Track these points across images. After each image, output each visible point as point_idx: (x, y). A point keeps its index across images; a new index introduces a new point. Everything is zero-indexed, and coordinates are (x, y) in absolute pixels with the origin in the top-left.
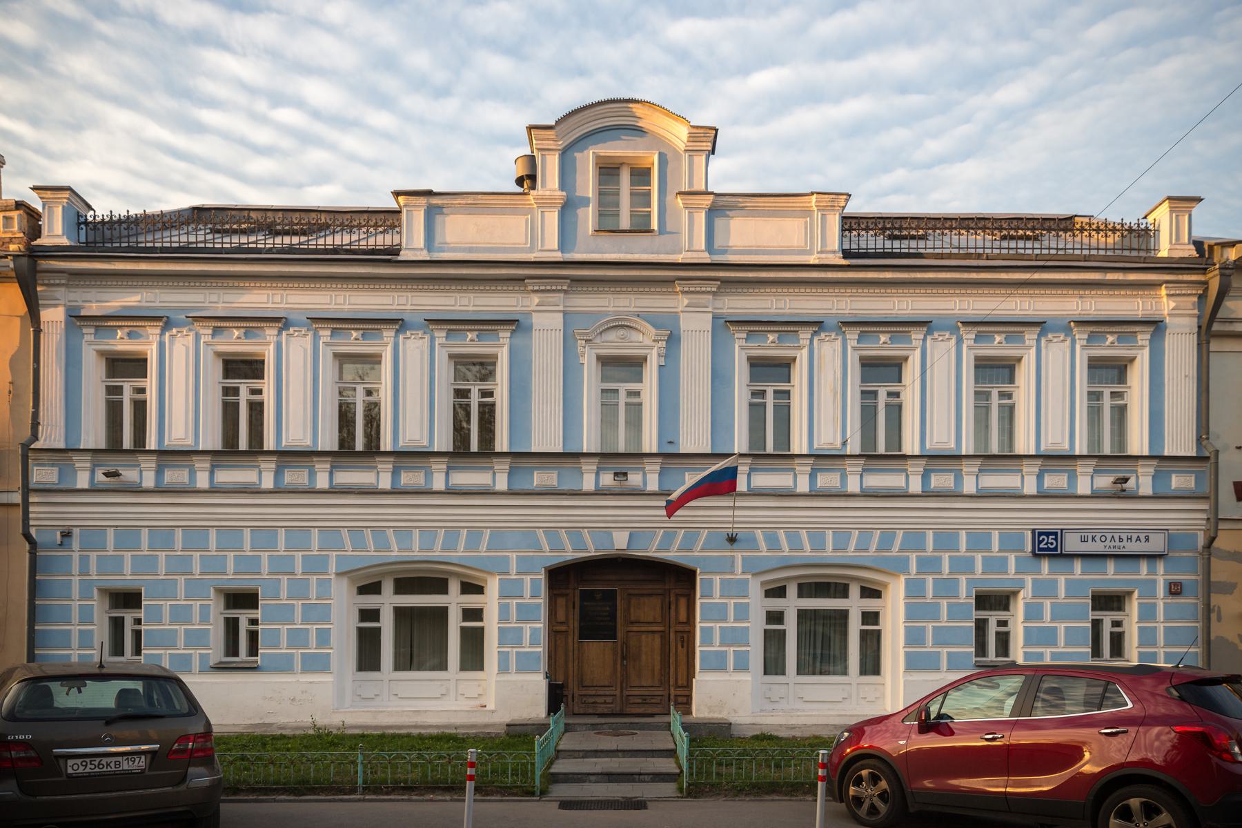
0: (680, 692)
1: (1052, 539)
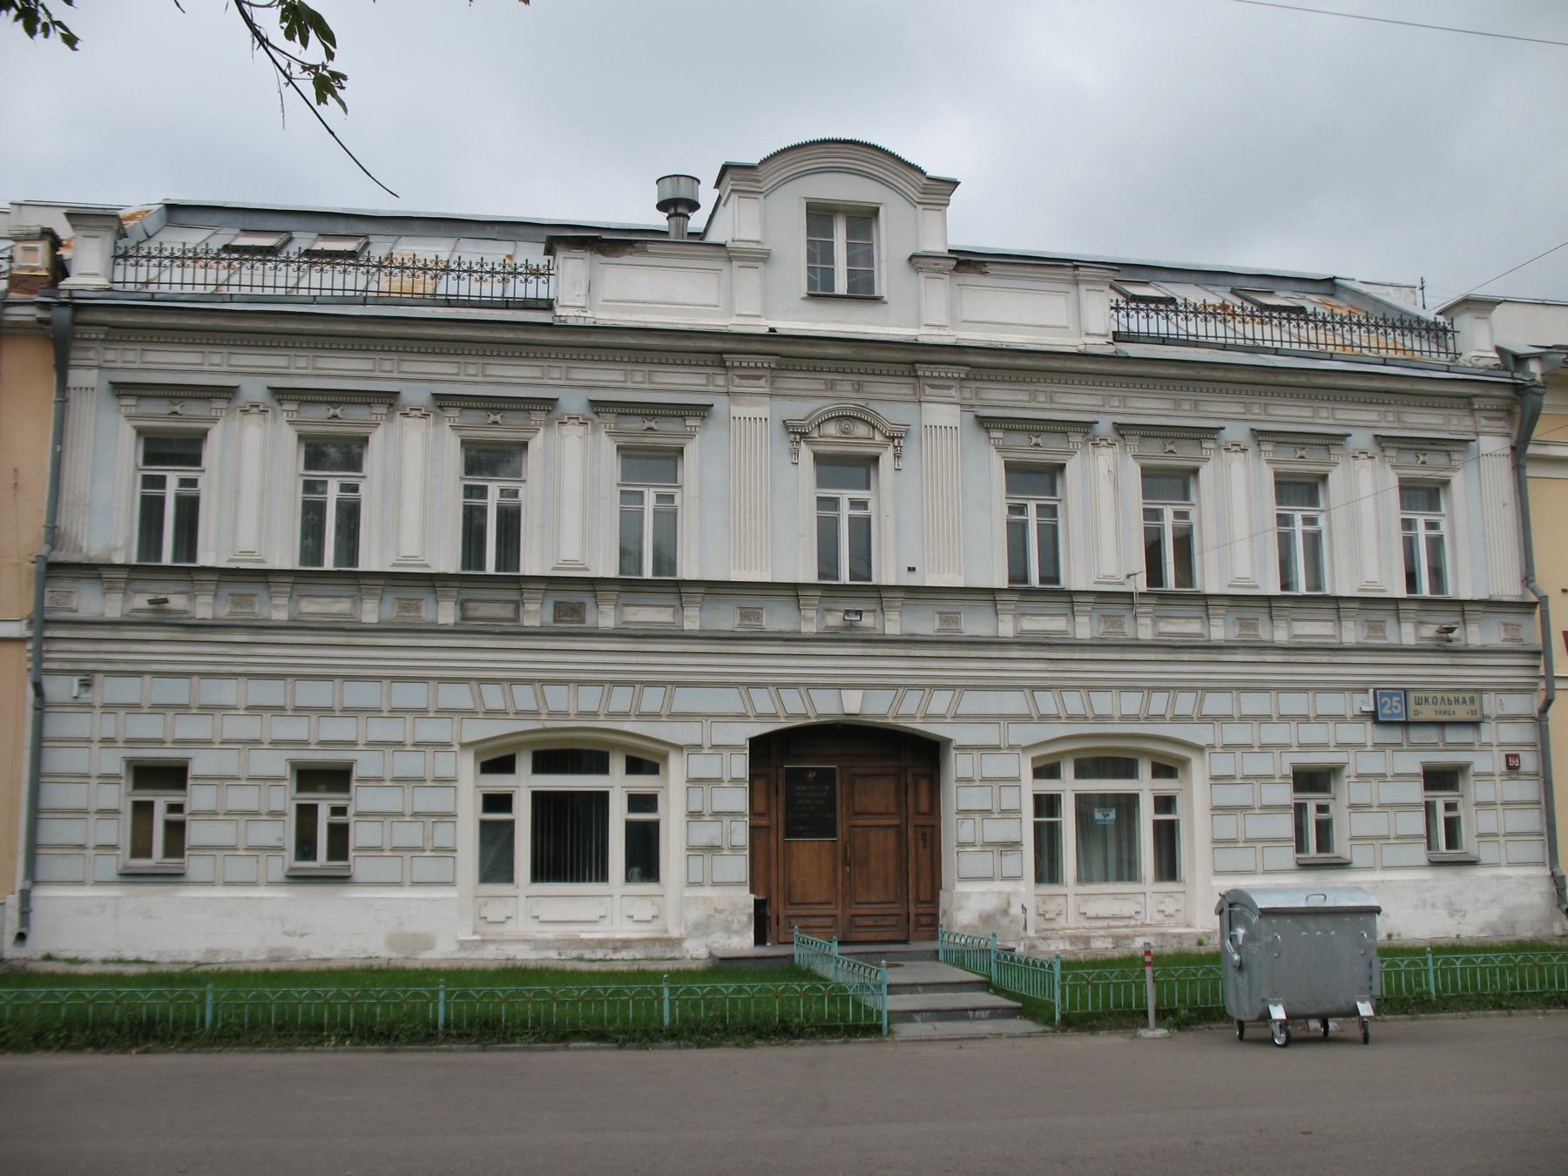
0: (923, 908)
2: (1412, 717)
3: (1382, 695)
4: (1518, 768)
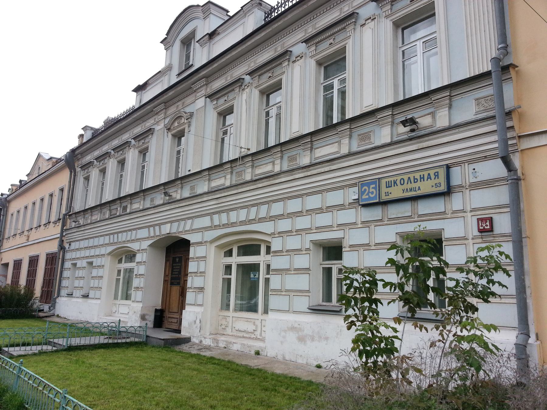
1: (373, 188)
2: (384, 198)
3: (363, 185)
4: (491, 230)
